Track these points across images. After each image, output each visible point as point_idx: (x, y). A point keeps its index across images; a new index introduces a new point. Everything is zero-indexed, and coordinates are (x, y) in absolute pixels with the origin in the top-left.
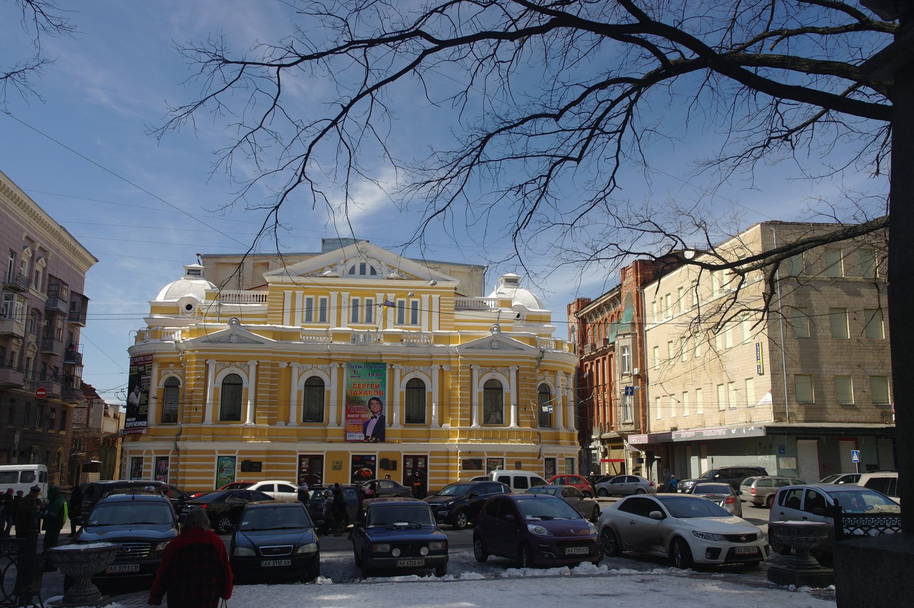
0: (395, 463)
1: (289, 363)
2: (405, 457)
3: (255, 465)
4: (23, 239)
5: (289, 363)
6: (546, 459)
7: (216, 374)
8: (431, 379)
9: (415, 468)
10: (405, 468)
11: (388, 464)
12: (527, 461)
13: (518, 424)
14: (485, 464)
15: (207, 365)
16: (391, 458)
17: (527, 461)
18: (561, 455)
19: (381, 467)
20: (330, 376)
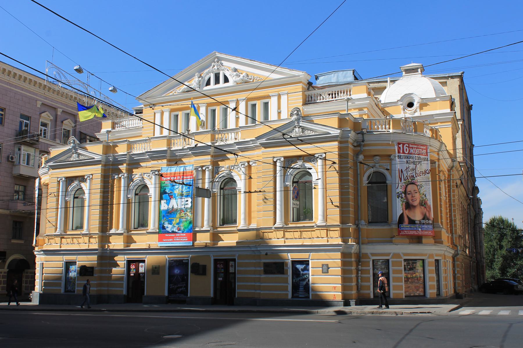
2: (216, 261)
4: (39, 106)
16: (202, 263)
19: (192, 272)
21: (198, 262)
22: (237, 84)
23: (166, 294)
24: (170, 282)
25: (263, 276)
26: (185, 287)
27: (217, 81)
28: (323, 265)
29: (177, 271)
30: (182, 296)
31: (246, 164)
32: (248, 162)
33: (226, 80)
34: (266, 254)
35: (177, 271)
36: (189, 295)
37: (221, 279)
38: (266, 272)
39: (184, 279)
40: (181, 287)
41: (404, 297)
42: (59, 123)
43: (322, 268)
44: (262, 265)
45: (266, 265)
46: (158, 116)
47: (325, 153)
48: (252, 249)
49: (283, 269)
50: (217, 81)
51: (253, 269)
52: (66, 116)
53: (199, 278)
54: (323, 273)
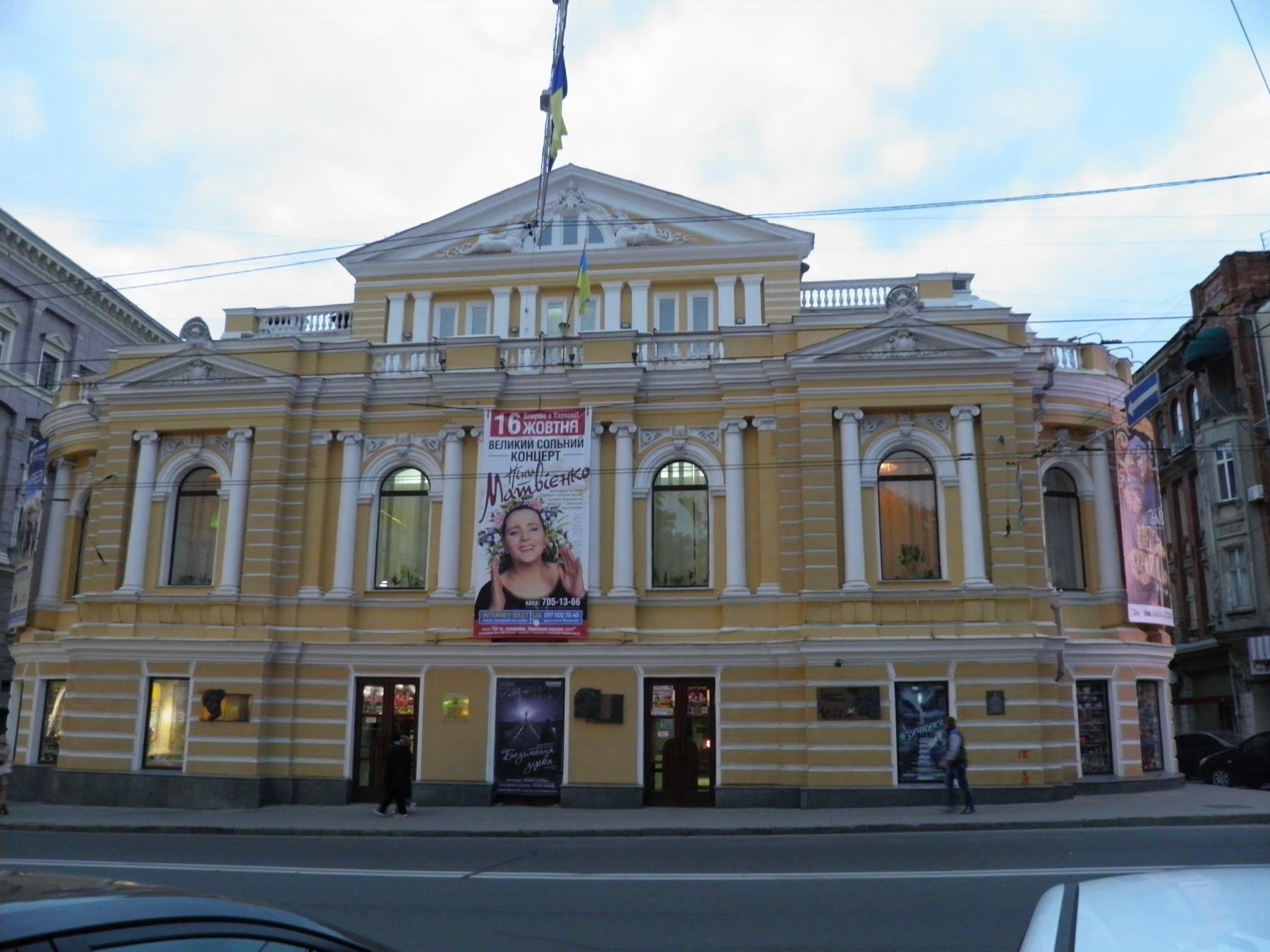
1: (335, 433)
2: (649, 683)
5: (335, 433)
6: (1081, 684)
7: (158, 467)
9: (682, 718)
10: (650, 722)
11: (599, 708)
12: (1023, 692)
13: (989, 576)
14: (889, 704)
15: (136, 445)
16: (608, 689)
17: (1023, 692)
18: (1125, 673)
19: (578, 714)
21: (596, 687)
22: (629, 245)
23: (490, 777)
24: (501, 742)
25: (816, 725)
26: (551, 756)
27: (570, 238)
28: (990, 695)
29: (525, 712)
30: (544, 784)
31: (744, 425)
32: (749, 420)
34: (838, 664)
35: (525, 712)
37: (666, 734)
38: (824, 714)
39: (550, 733)
40: (540, 758)
41: (1080, 775)
42: (35, 336)
44: (814, 695)
45: (825, 695)
46: (397, 310)
47: (979, 406)
48: (773, 652)
49: (878, 704)
50: (570, 238)
51: (772, 705)
52: (56, 325)
53: (600, 733)
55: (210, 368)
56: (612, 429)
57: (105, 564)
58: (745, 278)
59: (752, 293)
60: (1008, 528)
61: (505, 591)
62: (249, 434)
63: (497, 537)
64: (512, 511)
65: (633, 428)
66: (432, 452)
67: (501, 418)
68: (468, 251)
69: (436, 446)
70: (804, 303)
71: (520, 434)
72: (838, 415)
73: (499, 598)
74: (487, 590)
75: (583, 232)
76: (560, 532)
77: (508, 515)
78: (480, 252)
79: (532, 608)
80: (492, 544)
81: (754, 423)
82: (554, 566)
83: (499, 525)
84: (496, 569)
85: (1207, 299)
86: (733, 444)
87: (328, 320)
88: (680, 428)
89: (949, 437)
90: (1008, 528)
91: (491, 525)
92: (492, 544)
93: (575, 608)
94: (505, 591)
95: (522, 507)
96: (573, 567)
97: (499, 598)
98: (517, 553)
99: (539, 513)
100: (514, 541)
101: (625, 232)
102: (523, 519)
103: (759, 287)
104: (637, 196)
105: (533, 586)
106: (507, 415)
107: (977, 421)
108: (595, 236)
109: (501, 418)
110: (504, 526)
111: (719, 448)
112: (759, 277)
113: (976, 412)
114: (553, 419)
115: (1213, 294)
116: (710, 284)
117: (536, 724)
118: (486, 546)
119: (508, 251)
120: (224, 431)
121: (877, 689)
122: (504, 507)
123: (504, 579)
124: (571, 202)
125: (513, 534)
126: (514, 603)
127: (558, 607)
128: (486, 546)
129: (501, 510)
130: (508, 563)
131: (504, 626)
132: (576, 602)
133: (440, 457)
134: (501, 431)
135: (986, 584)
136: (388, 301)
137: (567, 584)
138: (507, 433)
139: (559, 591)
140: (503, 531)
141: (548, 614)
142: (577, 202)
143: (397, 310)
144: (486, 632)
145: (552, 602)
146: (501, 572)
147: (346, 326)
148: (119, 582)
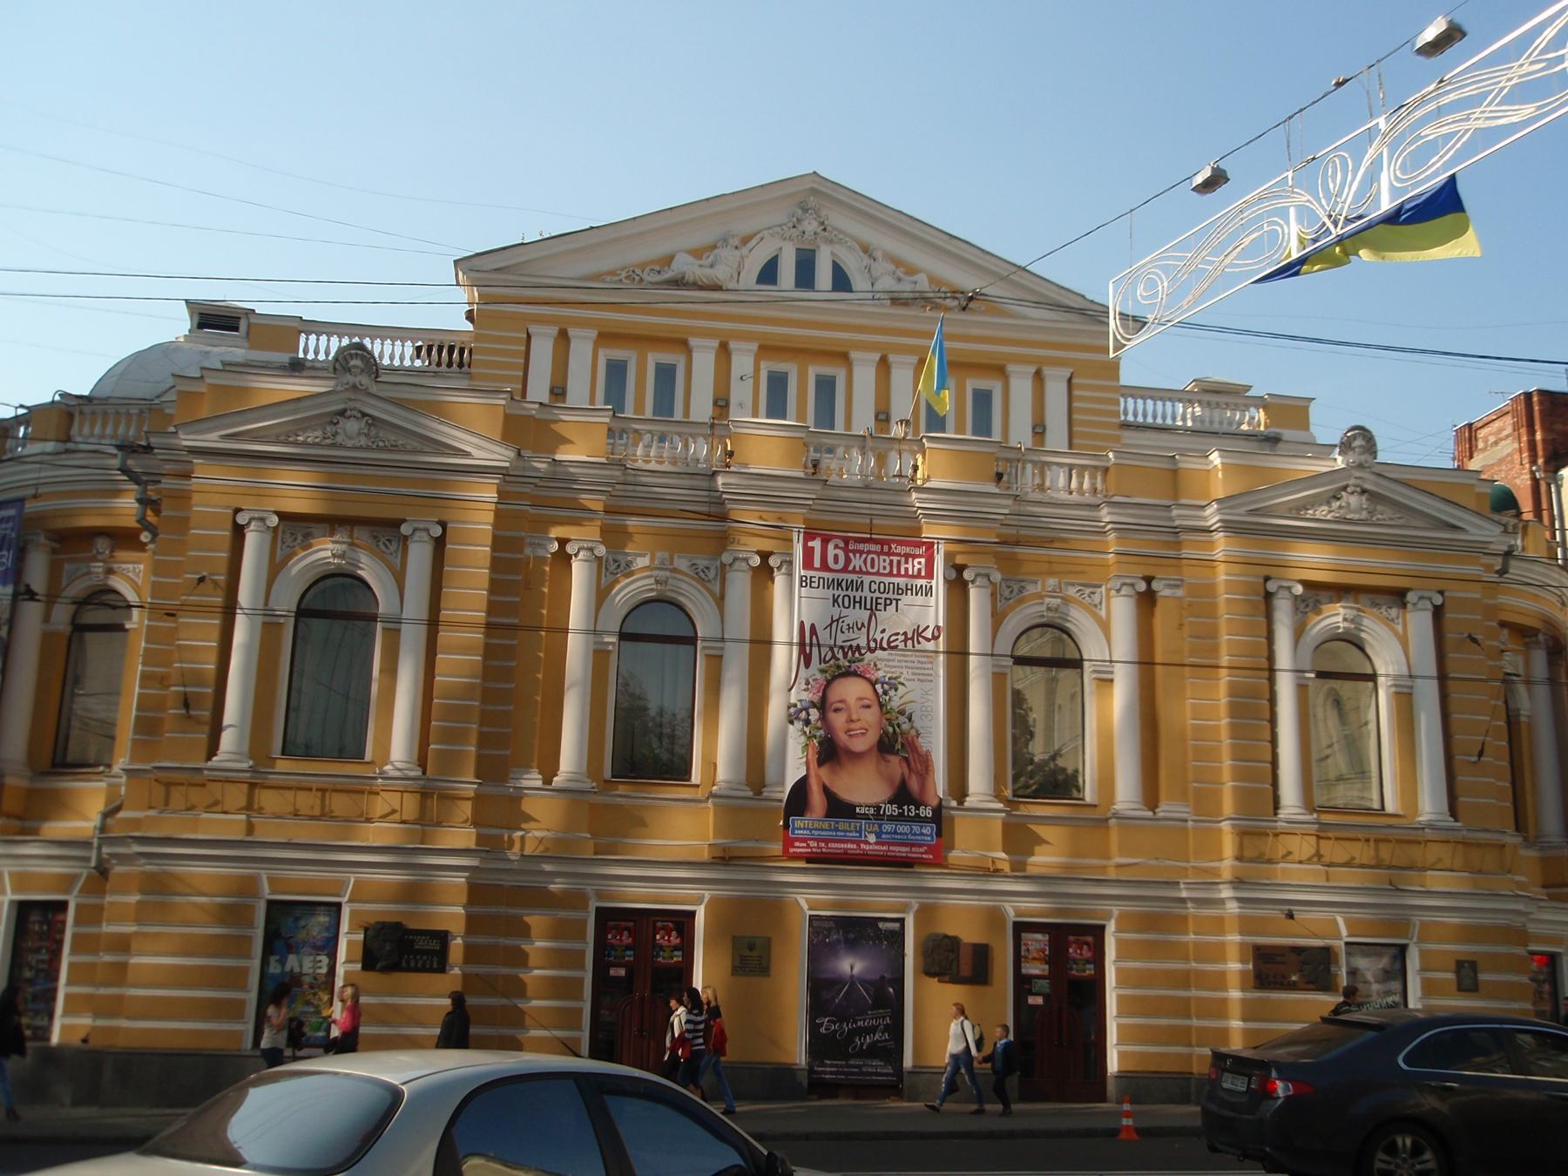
0: (982, 953)
3: (421, 944)
8: (1105, 627)
10: (1023, 984)
11: (954, 961)
15: (239, 532)
20: (720, 600)
24: (817, 1007)
26: (887, 1028)
27: (805, 277)
29: (850, 965)
31: (1142, 586)
32: (1149, 580)
33: (841, 281)
35: (850, 965)
36: (1113, 1064)
37: (1039, 1000)
39: (885, 996)
40: (872, 1030)
43: (1458, 972)
46: (542, 351)
47: (1441, 593)
50: (805, 277)
54: (1460, 989)
55: (374, 422)
56: (967, 575)
57: (189, 717)
58: (1047, 371)
59: (1056, 392)
60: (1481, 754)
61: (826, 791)
62: (437, 531)
63: (814, 714)
64: (834, 678)
65: (997, 577)
66: (702, 581)
67: (816, 544)
68: (658, 278)
69: (711, 575)
70: (1126, 414)
71: (845, 570)
72: (1271, 586)
73: (817, 800)
74: (801, 787)
75: (824, 277)
76: (902, 713)
77: (829, 683)
78: (678, 283)
79: (865, 817)
80: (807, 722)
81: (1155, 585)
82: (894, 760)
83: (816, 699)
84: (813, 758)
85: (1481, 445)
86: (1121, 611)
87: (409, 350)
88: (1052, 582)
89: (1400, 628)
90: (1481, 754)
91: (806, 696)
92: (807, 722)
93: (925, 820)
94: (826, 791)
95: (849, 673)
96: (923, 764)
97: (817, 800)
98: (842, 737)
99: (873, 685)
100: (838, 720)
101: (886, 283)
102: (851, 691)
103: (1065, 385)
104: (905, 233)
105: (864, 786)
106: (825, 541)
107: (1438, 612)
108: (841, 281)
109: (816, 544)
110: (824, 699)
111: (1103, 613)
112: (1067, 373)
113: (1438, 600)
114: (889, 554)
115: (1492, 439)
116: (999, 370)
117: (865, 983)
118: (799, 725)
119: (717, 288)
120: (397, 524)
121: (1327, 950)
122: (823, 671)
123: (824, 772)
124: (810, 226)
125: (836, 710)
126: (839, 808)
127: (901, 818)
128: (799, 725)
129: (818, 676)
130: (829, 752)
131: (826, 841)
132: (927, 812)
133: (717, 589)
134: (817, 564)
135: (1450, 822)
136: (529, 336)
137: (914, 785)
138: (825, 566)
139: (903, 795)
140: (822, 705)
141: (888, 827)
142: (819, 230)
143: (542, 351)
144: (799, 847)
145: (892, 810)
146: (820, 763)
147: (461, 365)
148: (213, 749)
